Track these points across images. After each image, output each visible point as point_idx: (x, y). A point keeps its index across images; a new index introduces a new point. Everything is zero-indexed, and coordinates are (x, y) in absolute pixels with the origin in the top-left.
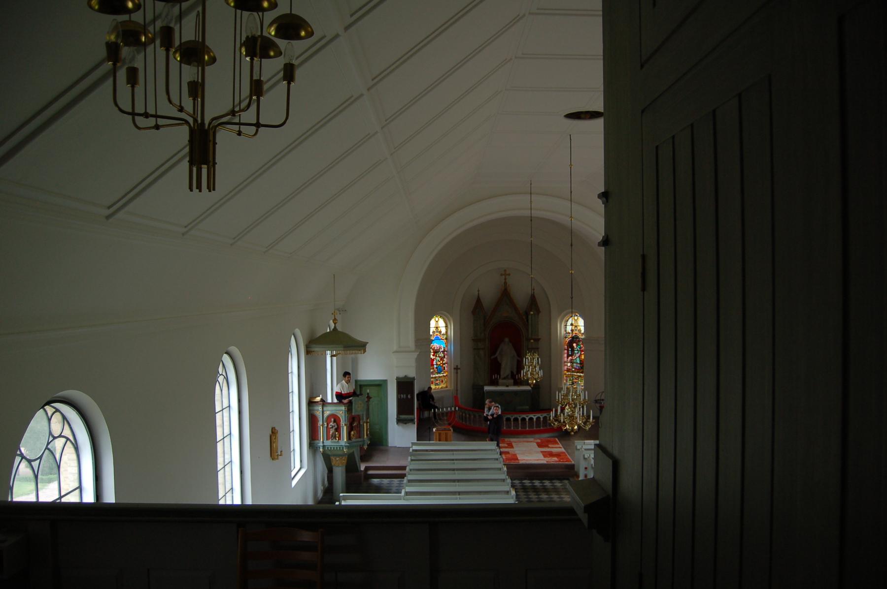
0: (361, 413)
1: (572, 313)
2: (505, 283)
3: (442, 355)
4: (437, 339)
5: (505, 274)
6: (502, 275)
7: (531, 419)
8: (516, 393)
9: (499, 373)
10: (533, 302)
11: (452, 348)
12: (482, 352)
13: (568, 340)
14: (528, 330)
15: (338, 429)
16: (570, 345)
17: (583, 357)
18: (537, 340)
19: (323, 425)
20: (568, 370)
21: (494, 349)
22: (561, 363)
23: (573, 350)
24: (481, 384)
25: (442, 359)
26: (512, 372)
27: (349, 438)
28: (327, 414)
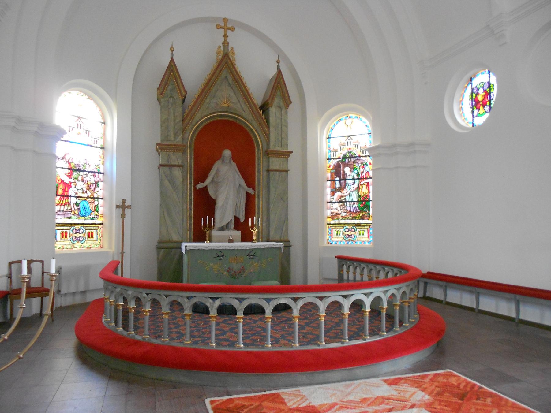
2: (225, 44)
3: (91, 179)
5: (226, 26)
7: (357, 305)
9: (212, 215)
10: (278, 84)
11: (112, 166)
13: (333, 163)
14: (268, 137)
18: (287, 154)
20: (333, 217)
21: (201, 172)
22: (321, 204)
24: (175, 237)
26: (237, 219)
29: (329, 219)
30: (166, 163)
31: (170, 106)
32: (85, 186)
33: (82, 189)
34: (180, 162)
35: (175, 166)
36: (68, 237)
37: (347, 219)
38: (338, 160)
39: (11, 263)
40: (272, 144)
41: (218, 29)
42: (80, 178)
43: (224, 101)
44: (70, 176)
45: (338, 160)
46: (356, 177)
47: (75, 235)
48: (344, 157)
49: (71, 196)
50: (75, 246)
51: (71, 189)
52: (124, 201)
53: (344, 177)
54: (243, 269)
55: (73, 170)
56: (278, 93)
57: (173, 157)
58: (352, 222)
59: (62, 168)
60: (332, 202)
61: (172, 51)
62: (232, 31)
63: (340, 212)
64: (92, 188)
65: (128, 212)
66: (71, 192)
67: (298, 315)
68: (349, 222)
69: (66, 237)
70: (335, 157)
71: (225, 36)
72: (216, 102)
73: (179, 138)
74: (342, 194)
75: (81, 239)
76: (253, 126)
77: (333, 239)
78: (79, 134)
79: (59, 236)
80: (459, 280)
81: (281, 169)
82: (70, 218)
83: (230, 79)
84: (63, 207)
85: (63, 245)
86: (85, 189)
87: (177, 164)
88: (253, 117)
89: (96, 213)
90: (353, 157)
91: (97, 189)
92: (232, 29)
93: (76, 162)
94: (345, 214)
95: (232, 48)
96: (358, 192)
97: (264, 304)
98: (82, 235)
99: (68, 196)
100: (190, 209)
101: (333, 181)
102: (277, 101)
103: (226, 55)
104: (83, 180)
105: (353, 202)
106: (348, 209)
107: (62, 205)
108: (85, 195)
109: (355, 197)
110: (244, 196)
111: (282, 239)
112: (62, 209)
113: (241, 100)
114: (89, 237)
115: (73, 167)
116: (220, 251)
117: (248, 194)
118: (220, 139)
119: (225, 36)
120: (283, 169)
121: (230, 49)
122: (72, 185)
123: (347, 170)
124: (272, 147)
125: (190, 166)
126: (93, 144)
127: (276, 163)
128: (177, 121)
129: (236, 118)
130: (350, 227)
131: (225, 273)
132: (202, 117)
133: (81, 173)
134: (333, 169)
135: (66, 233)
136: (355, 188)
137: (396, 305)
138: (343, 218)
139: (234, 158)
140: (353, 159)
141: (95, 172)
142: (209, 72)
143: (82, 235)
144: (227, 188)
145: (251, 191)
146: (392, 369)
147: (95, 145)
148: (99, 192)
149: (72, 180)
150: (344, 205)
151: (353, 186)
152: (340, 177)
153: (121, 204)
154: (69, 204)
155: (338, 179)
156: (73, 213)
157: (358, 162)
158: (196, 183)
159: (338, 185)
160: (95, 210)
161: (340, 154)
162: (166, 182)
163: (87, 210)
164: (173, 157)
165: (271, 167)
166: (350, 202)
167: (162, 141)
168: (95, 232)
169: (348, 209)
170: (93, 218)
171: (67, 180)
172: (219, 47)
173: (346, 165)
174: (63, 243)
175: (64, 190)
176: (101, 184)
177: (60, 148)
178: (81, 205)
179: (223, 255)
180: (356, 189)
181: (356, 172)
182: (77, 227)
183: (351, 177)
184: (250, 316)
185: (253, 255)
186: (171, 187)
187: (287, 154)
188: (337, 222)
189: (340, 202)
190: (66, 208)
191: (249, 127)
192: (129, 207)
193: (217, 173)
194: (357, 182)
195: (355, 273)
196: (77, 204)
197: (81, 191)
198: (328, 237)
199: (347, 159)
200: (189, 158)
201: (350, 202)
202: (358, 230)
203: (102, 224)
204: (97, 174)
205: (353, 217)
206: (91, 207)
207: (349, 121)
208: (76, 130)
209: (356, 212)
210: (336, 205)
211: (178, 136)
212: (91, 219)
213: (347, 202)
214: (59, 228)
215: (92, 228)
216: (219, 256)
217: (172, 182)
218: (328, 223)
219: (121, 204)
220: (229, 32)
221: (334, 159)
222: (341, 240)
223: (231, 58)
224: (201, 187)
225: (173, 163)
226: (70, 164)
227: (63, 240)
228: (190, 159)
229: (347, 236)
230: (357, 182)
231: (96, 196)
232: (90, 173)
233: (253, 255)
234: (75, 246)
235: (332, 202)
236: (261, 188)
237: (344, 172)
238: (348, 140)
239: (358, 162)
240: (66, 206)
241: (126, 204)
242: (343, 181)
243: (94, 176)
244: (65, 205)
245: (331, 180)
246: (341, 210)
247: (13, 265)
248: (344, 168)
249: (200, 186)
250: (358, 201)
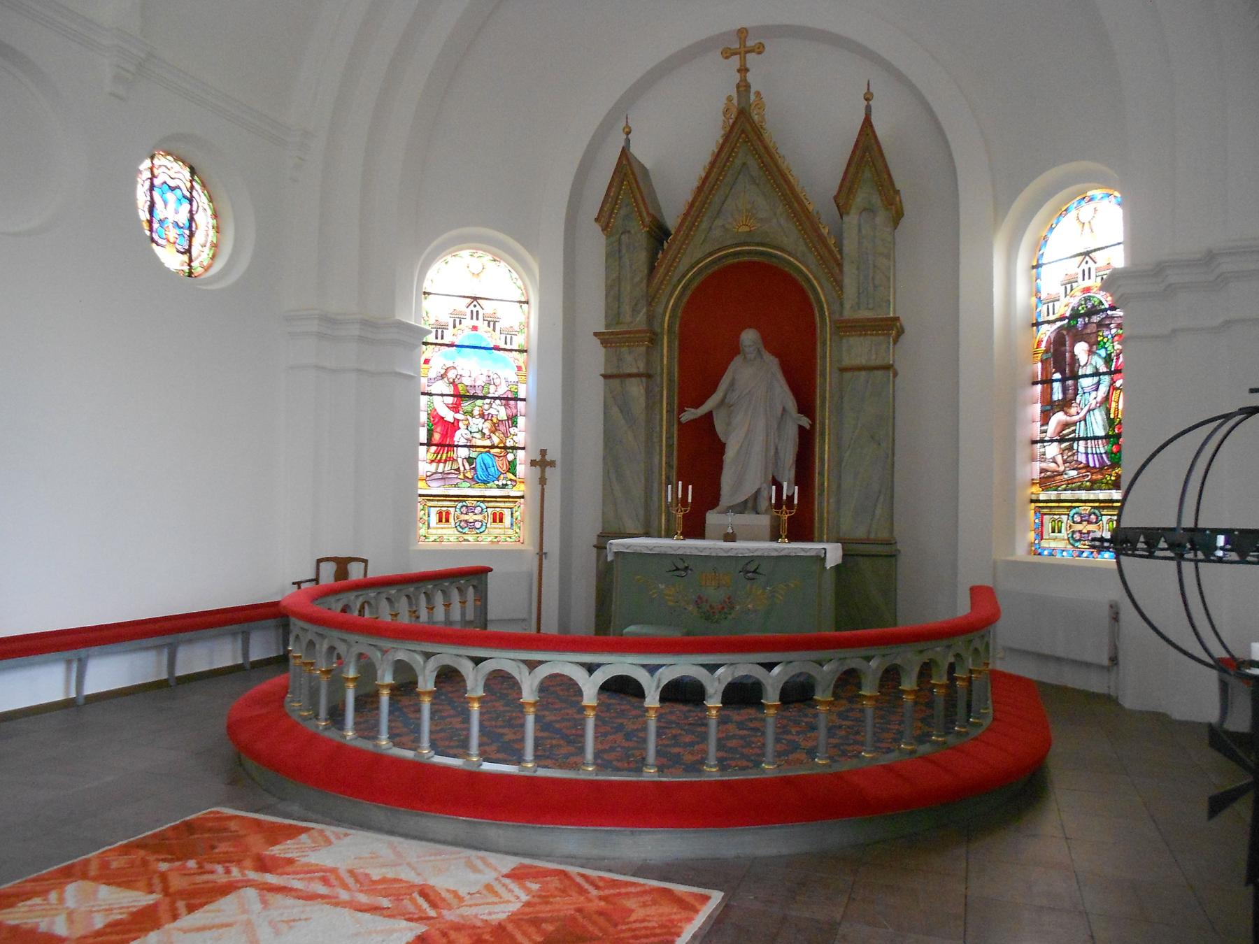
1: (1074, 187)
3: (501, 412)
5: (742, 47)
10: (867, 152)
12: (636, 390)
13: (1047, 332)
14: (839, 285)
16: (1059, 358)
17: (1119, 402)
20: (1047, 480)
23: (1072, 374)
29: (1036, 489)
30: (615, 372)
31: (624, 251)
32: (488, 424)
33: (481, 431)
34: (641, 367)
35: (630, 375)
36: (451, 520)
37: (1080, 488)
38: (1059, 324)
39: (319, 561)
40: (847, 306)
41: (727, 58)
42: (476, 412)
43: (749, 217)
44: (455, 408)
45: (1059, 324)
46: (1103, 369)
47: (466, 517)
48: (1075, 315)
49: (458, 446)
50: (466, 537)
51: (458, 434)
52: (543, 452)
53: (1072, 371)
54: (729, 604)
55: (460, 397)
56: (867, 174)
57: (629, 358)
58: (1092, 495)
59: (442, 395)
60: (1042, 441)
61: (628, 133)
62: (760, 53)
63: (1062, 468)
64: (502, 428)
65: (554, 476)
66: (459, 437)
67: (480, 692)
68: (1083, 495)
69: (447, 521)
70: (1052, 317)
71: (743, 70)
72: (723, 226)
73: (641, 317)
74: (1068, 419)
75: (478, 525)
76: (807, 267)
77: (1044, 544)
78: (475, 328)
79: (434, 518)
80: (198, 620)
81: (873, 363)
82: (456, 486)
83: (753, 164)
84: (441, 465)
86: (486, 431)
87: (635, 371)
88: (806, 244)
89: (510, 476)
90: (1097, 312)
91: (512, 430)
92: (760, 49)
93: (467, 381)
94: (1073, 473)
95: (758, 94)
96: (1108, 413)
97: (642, 677)
98: (479, 517)
99: (452, 446)
100: (669, 465)
101: (1047, 382)
102: (864, 195)
104: (482, 416)
105: (1096, 438)
106: (1082, 458)
107: (439, 461)
108: (488, 443)
109: (1097, 425)
110: (791, 433)
111: (872, 536)
112: (440, 470)
113: (780, 209)
114: (494, 521)
115: (462, 392)
116: (682, 557)
117: (801, 428)
118: (744, 303)
119: (743, 70)
120: (879, 362)
121: (752, 97)
122: (461, 424)
123: (1081, 349)
124: (848, 314)
125: (670, 373)
126: (502, 346)
127: (859, 350)
128: (637, 279)
129: (771, 255)
130: (1086, 509)
131: (690, 608)
132: (691, 260)
133: (479, 402)
134: (1047, 351)
135: (448, 513)
136: (1099, 399)
137: (347, 679)
138: (1071, 485)
139: (771, 344)
140: (1095, 319)
141: (507, 399)
142: (782, 151)
143: (479, 517)
144: (753, 415)
145: (805, 422)
146: (595, 852)
147: (508, 347)
148: (519, 435)
149: (459, 416)
150: (1071, 448)
151: (1094, 394)
152: (1063, 373)
153: (538, 458)
154: (454, 460)
155: (1057, 376)
156: (461, 476)
157: (1108, 326)
158: (681, 411)
159: (1057, 395)
160: (508, 470)
161: (1063, 308)
162: (615, 410)
163: (492, 470)
164: (629, 358)
165: (847, 362)
166: (1086, 439)
167: (607, 326)
168: (507, 513)
169: (1082, 458)
170: (504, 486)
171: (449, 416)
172: (729, 99)
173: (1079, 337)
174: (440, 532)
175: (444, 436)
176: (521, 421)
177: (438, 359)
178: (478, 460)
179: (687, 568)
180: (1101, 403)
181: (1103, 353)
182: (470, 502)
183: (1089, 370)
184: (680, 708)
185: (754, 572)
186: (623, 421)
187: (890, 328)
188: (1053, 495)
189: (1061, 441)
190: (448, 466)
191: (801, 272)
192: (552, 464)
193: (732, 384)
194: (1106, 380)
195: (431, 609)
196: (470, 460)
197: (478, 435)
198: (1032, 536)
199: (1080, 320)
200: (667, 354)
201: (1086, 439)
202: (1105, 519)
203: (522, 497)
204: (512, 402)
205: (1093, 482)
206: (501, 464)
207: (1086, 210)
208: (468, 323)
209: (1101, 468)
210: (1052, 450)
211: (639, 312)
212: (498, 487)
213: (1079, 439)
214: (435, 503)
215: (502, 505)
216: (678, 569)
217: (625, 409)
218: (1034, 497)
219: (538, 458)
221: (1049, 322)
222: (1061, 545)
223: (756, 118)
224: (692, 417)
225: (628, 371)
226: (455, 386)
227: (441, 525)
228: (670, 359)
229: (1077, 536)
230: (1106, 380)
231: (509, 443)
232: (498, 402)
233: (754, 572)
234: (466, 537)
235: (1042, 441)
237: (1073, 355)
238: (471, 307)
239: (1108, 326)
240: (449, 464)
241: (548, 458)
242: (1070, 382)
243: (507, 406)
244: (445, 461)
245: (1042, 382)
246: (1065, 462)
247: (322, 565)
248: (1073, 346)
249: (690, 414)
250: (1107, 437)
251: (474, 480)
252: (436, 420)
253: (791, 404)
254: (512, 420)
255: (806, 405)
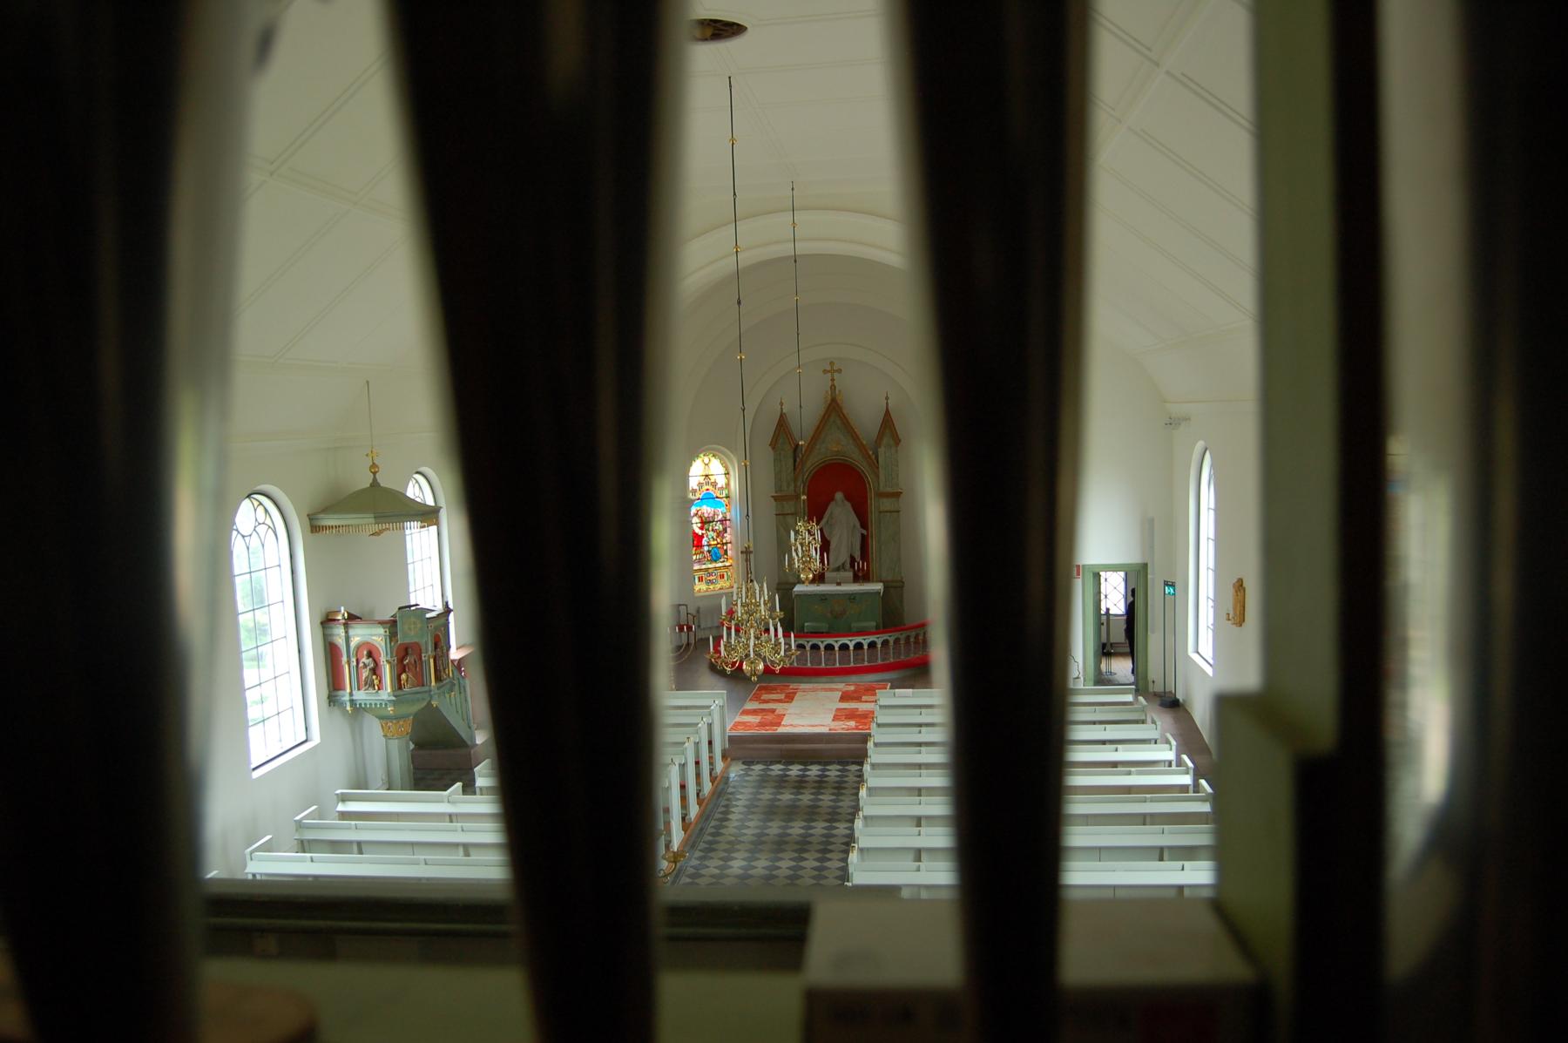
0: (422, 642)
2: (833, 387)
3: (719, 527)
4: (708, 498)
5: (832, 370)
6: (825, 372)
8: (852, 597)
10: (887, 422)
15: (375, 671)
18: (897, 495)
19: (349, 663)
25: (720, 534)
27: (398, 685)
28: (355, 641)
43: (835, 445)
55: (705, 522)
66: (704, 542)
85: (700, 587)
103: (834, 400)
127: (886, 504)
132: (812, 463)
139: (848, 498)
148: (728, 537)
171: (700, 532)
206: (721, 552)
220: (836, 375)
236: (873, 528)
251: (713, 561)
252: (695, 535)
253: (858, 524)
254: (725, 530)
255: (864, 525)
